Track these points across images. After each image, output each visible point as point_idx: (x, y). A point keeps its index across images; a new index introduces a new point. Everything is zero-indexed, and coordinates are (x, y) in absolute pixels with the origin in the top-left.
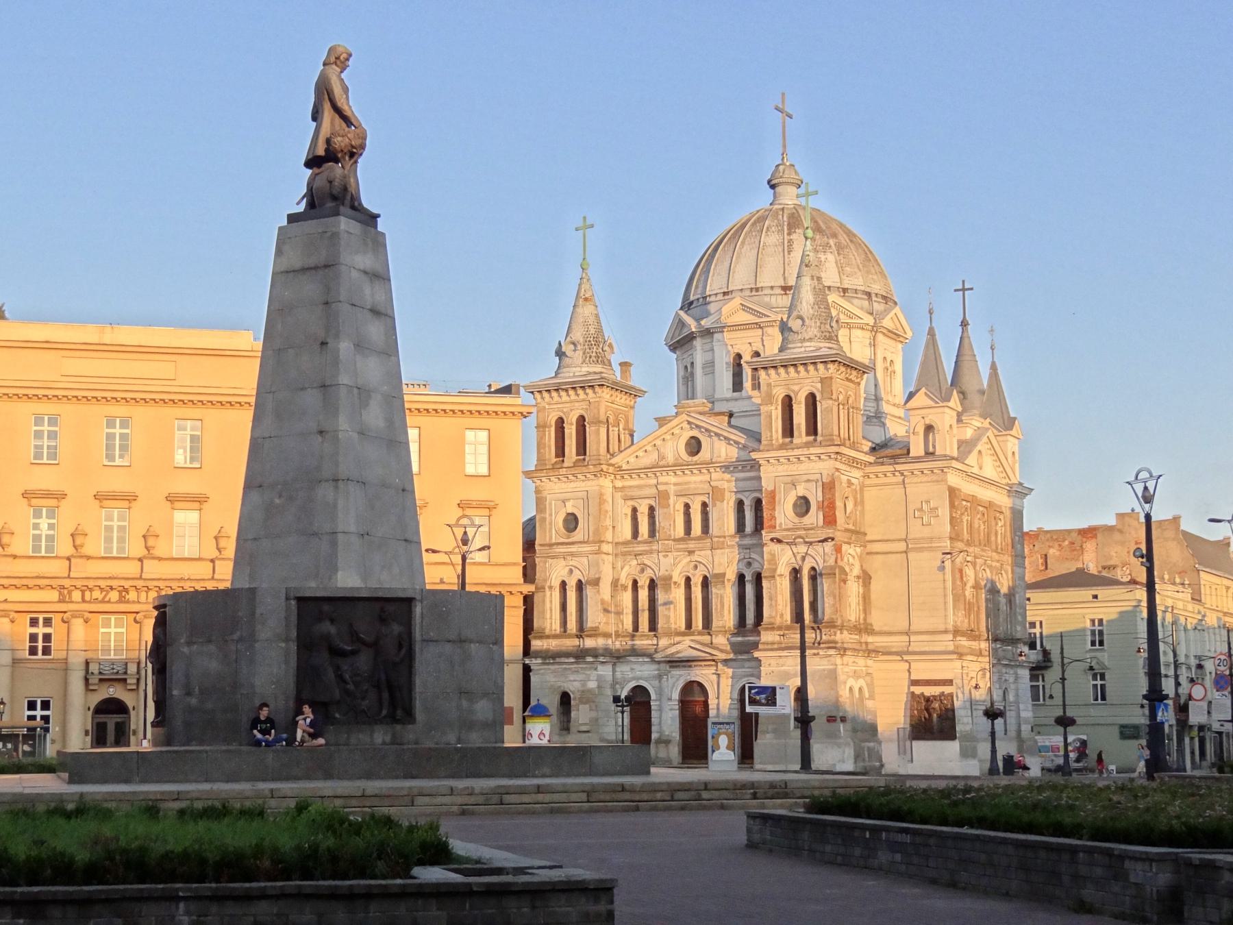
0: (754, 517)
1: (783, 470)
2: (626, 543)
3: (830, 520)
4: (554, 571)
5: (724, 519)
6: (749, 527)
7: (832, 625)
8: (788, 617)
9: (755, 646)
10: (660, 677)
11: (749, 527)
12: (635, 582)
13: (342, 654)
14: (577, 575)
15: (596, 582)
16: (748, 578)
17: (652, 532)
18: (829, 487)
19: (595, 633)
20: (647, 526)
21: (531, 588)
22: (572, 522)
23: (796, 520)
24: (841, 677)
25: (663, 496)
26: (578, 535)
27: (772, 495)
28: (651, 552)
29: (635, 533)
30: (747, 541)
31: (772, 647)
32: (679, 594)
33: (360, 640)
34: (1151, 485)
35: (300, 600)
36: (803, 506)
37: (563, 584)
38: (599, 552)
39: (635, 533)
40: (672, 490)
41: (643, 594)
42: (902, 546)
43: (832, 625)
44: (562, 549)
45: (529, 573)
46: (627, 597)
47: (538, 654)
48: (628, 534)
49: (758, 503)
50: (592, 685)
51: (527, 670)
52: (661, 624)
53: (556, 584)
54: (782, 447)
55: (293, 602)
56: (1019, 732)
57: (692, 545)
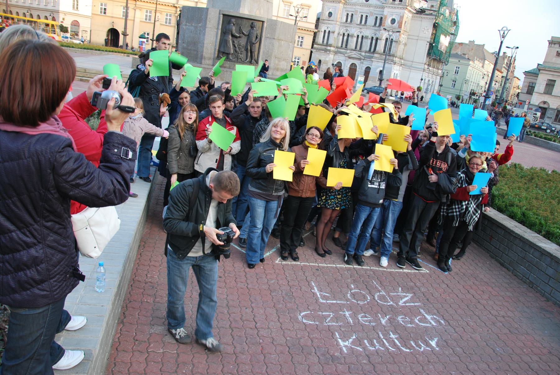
0: (380, 22)
1: (390, 10)
2: (344, 23)
3: (400, 27)
4: (323, 28)
5: (371, 21)
6: (377, 25)
7: (393, 56)
8: (382, 51)
9: (372, 57)
10: (345, 61)
11: (377, 25)
12: (344, 34)
13: (236, 37)
14: (329, 29)
15: (334, 32)
16: (374, 38)
17: (351, 21)
18: (402, 17)
19: (330, 46)
20: (350, 18)
21: (316, 31)
22: (330, 14)
23: (391, 25)
24: (393, 70)
25: (356, 11)
26: (332, 18)
27: (386, 17)
28: (350, 27)
29: (347, 21)
30: (376, 28)
31: (376, 58)
32: (355, 39)
33: (243, 34)
34: (506, 32)
35: (224, 15)
36: (393, 21)
37: (325, 31)
38: (336, 24)
39: (347, 21)
40: (359, 11)
41: (345, 38)
42: (417, 38)
43: (393, 56)
44: (327, 22)
45: (317, 26)
46: (341, 37)
47: (315, 48)
48: (345, 20)
49: (382, 18)
50: (327, 59)
51: (311, 52)
52: (348, 46)
53: (323, 31)
54: (392, 4)
55: (222, 16)
56: (433, 92)
57: (361, 27)
